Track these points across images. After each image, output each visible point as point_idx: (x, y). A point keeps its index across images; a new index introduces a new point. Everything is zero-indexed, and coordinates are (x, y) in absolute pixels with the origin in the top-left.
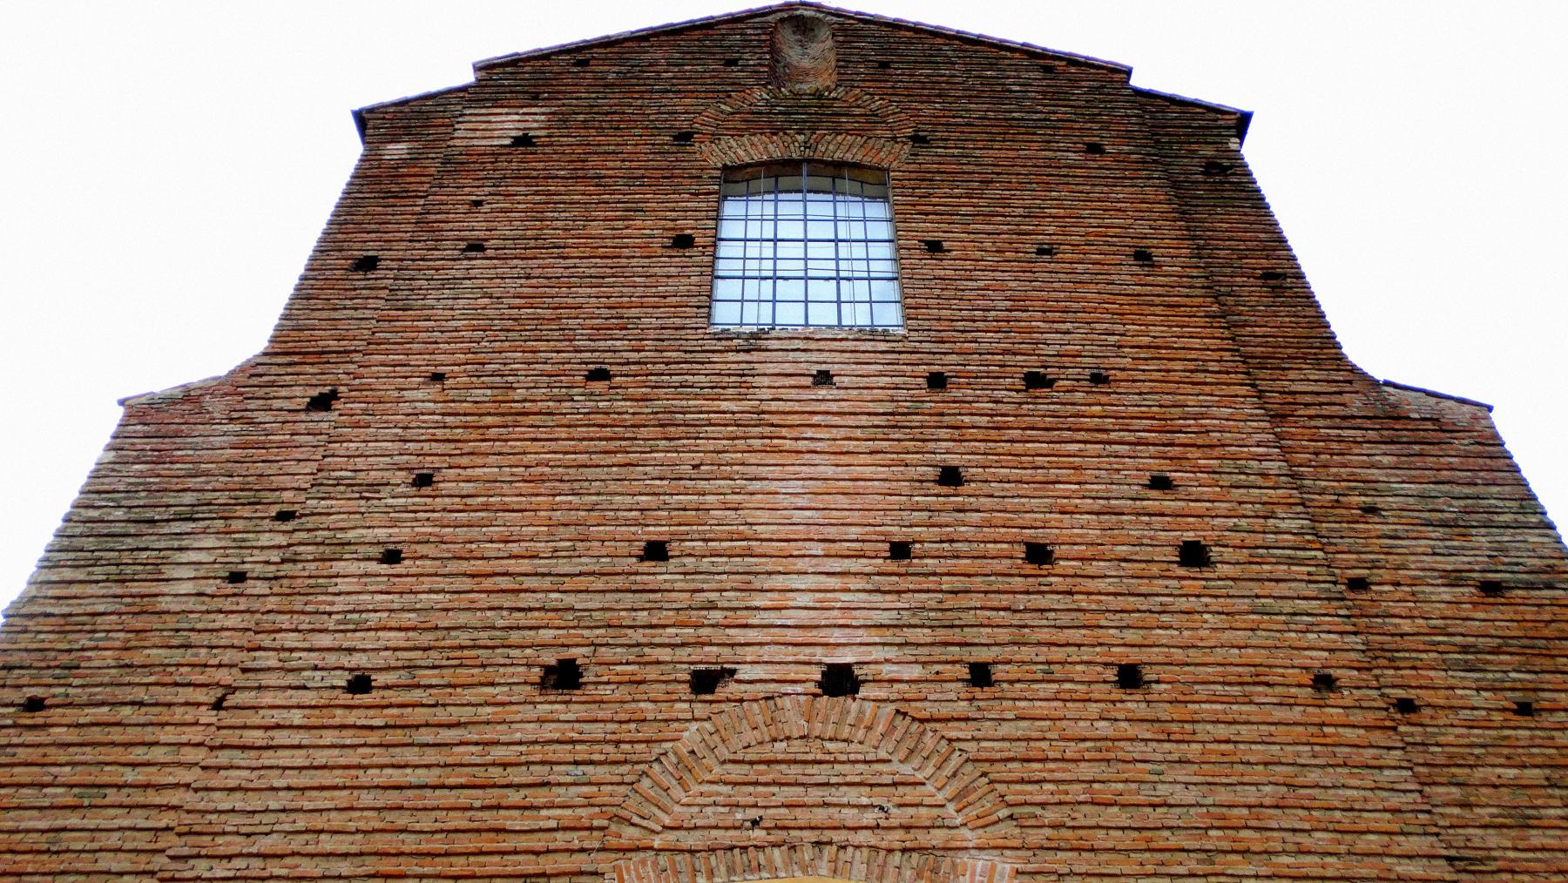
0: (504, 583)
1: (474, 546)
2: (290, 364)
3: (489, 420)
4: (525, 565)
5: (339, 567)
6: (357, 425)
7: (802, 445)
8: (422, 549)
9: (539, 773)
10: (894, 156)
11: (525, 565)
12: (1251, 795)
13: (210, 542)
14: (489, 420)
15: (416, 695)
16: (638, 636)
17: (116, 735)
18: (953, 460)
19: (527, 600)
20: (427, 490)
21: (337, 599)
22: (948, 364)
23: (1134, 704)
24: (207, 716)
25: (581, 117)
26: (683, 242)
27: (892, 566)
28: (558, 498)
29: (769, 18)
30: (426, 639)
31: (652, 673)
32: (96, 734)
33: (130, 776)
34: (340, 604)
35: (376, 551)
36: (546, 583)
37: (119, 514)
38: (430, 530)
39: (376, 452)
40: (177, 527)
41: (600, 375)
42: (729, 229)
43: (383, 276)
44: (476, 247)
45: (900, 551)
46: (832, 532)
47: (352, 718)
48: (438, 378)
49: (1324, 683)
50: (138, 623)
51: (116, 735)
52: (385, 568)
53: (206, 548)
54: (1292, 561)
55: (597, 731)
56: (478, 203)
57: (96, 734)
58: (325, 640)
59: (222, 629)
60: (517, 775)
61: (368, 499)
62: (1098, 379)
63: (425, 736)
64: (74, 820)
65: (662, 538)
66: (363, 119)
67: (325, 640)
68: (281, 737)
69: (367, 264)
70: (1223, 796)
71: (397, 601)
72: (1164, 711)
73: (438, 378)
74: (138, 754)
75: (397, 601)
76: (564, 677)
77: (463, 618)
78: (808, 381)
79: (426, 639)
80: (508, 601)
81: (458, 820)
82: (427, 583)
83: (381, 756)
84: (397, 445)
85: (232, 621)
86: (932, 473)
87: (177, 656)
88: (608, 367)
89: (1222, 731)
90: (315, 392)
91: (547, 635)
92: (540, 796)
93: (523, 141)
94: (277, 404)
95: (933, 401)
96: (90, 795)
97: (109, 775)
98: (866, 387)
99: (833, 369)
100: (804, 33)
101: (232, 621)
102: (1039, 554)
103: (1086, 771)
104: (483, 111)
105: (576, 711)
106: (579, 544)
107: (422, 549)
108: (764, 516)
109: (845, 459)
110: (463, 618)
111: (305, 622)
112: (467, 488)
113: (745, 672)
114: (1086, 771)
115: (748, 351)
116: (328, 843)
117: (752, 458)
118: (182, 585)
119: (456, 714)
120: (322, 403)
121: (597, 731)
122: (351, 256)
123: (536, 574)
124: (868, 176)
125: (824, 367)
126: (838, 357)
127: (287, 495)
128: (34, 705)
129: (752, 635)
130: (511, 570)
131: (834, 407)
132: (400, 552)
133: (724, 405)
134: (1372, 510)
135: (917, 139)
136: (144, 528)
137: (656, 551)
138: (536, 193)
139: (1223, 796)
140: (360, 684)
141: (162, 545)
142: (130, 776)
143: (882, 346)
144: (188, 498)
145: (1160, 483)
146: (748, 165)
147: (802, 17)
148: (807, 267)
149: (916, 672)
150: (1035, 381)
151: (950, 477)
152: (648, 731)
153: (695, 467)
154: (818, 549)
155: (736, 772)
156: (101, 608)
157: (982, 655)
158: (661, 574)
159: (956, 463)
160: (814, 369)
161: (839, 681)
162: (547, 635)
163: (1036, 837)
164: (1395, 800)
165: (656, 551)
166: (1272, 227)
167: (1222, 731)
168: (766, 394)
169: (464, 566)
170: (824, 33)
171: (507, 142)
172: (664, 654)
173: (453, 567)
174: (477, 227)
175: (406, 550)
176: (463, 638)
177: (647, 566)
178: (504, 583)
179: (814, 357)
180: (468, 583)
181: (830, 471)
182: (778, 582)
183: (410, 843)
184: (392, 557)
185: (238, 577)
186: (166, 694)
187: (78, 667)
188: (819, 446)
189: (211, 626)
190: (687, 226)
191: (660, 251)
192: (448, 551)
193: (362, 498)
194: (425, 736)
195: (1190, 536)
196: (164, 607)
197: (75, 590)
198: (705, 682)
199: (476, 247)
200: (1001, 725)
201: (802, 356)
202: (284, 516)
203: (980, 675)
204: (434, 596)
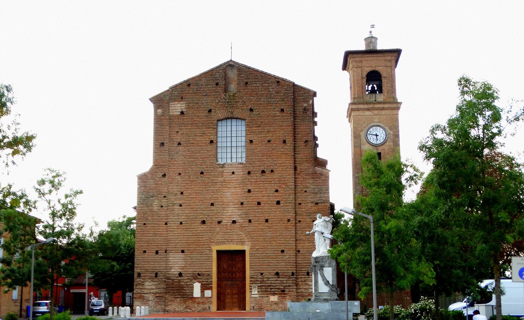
0: (194, 209)
3: (188, 182)
4: (197, 207)
6: (171, 183)
7: (230, 186)
9: (202, 234)
11: (197, 207)
12: (277, 235)
14: (188, 182)
15: (187, 225)
16: (211, 217)
17: (155, 228)
18: (250, 188)
19: (198, 212)
23: (266, 224)
24: (165, 226)
25: (191, 105)
26: (212, 142)
27: (241, 206)
30: (187, 217)
31: (213, 222)
32: (153, 228)
33: (159, 233)
34: (177, 212)
36: (200, 209)
39: (176, 189)
40: (152, 198)
41: (202, 173)
42: (219, 134)
43: (166, 146)
45: (242, 204)
46: (233, 201)
47: (182, 227)
48: (180, 174)
49: (289, 220)
50: (152, 213)
51: (155, 228)
53: (156, 203)
54: (290, 203)
55: (208, 229)
56: (178, 132)
57: (153, 228)
58: (176, 217)
60: (200, 234)
62: (272, 171)
63: (190, 230)
64: (154, 238)
66: (150, 99)
67: (176, 217)
68: (175, 230)
69: (162, 144)
70: (274, 235)
71: (183, 212)
72: (269, 225)
74: (159, 230)
75: (183, 212)
76: (204, 222)
77: (191, 214)
78: (231, 174)
79: (187, 217)
80: (196, 212)
81: (195, 239)
83: (186, 232)
85: (163, 213)
86: (247, 190)
87: (158, 218)
89: (275, 227)
91: (201, 217)
92: (202, 237)
93: (182, 113)
95: (248, 177)
96: (155, 235)
97: (156, 233)
101: (163, 213)
102: (259, 203)
103: (260, 232)
105: (205, 227)
110: (191, 214)
111: (173, 215)
113: (224, 221)
114: (260, 232)
116: (182, 242)
117: (224, 189)
118: (155, 208)
119: (192, 227)
121: (208, 229)
122: (160, 145)
126: (235, 168)
128: (145, 224)
129: (224, 217)
133: (220, 179)
134: (306, 191)
135: (251, 110)
137: (212, 204)
139: (274, 235)
140: (181, 223)
142: (159, 233)
143: (242, 166)
145: (277, 191)
148: (232, 142)
149: (242, 221)
150: (263, 172)
151: (249, 191)
152: (213, 229)
154: (232, 204)
155: (222, 234)
157: (250, 218)
158: (213, 208)
161: (234, 222)
162: (201, 217)
163: (253, 240)
164: (292, 235)
165: (212, 204)
167: (275, 227)
169: (189, 207)
172: (214, 219)
174: (178, 138)
176: (191, 217)
177: (212, 207)
178: (194, 209)
179: (232, 169)
180: (190, 209)
181: (233, 191)
182: (227, 209)
183: (191, 242)
184: (181, 206)
185: (162, 206)
186: (159, 223)
190: (212, 138)
194: (190, 230)
195: (278, 200)
198: (219, 222)
199: (179, 144)
200: (251, 228)
202: (165, 197)
203: (250, 221)
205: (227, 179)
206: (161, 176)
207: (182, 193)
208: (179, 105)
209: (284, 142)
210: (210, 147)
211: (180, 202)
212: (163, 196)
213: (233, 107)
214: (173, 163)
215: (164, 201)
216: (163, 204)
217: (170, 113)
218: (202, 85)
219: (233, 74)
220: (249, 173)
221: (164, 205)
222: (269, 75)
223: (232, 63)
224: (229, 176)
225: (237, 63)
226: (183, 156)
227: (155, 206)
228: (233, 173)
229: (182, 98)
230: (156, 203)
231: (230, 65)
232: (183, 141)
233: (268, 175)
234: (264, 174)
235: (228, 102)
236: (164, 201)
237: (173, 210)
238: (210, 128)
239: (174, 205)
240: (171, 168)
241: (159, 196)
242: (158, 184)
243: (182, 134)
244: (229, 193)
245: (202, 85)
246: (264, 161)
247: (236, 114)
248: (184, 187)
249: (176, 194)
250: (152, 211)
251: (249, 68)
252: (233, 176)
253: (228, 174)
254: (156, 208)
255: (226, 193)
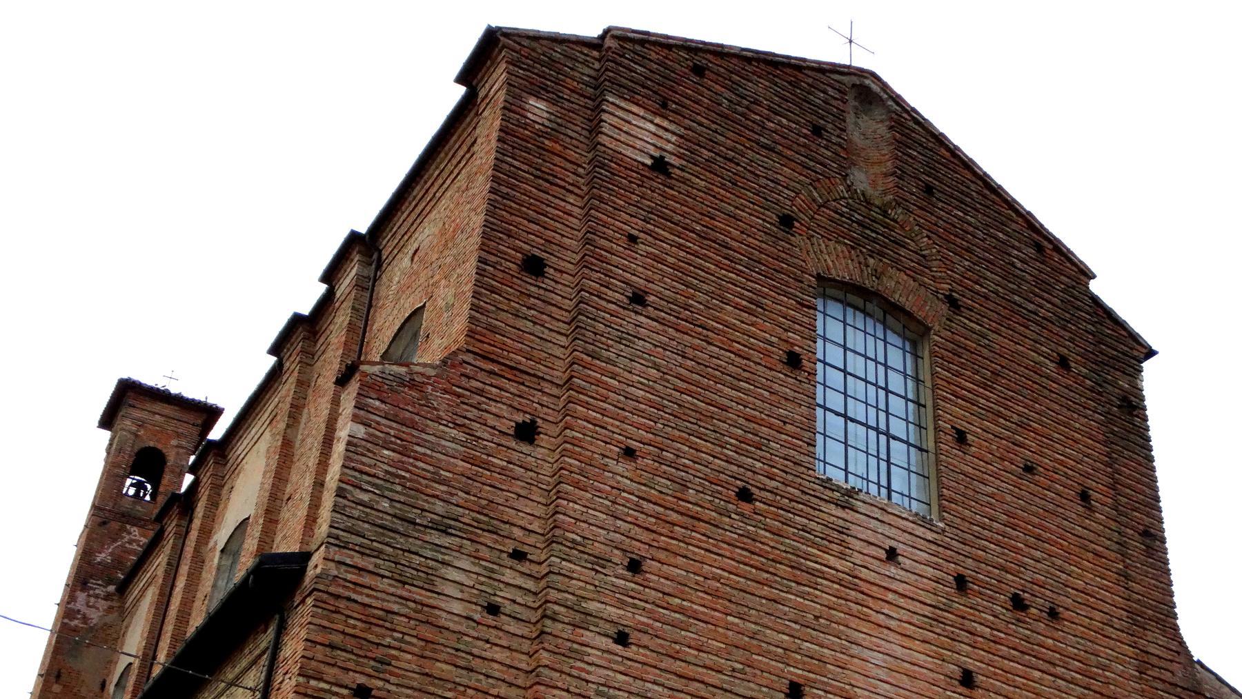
1: (678, 647)
2: (491, 372)
3: (674, 517)
4: (714, 678)
5: (587, 636)
6: (576, 484)
8: (645, 640)
10: (932, 311)
11: (714, 678)
13: (465, 564)
14: (674, 517)
18: (971, 664)
20: (638, 578)
21: (592, 669)
22: (968, 567)
28: (729, 618)
29: (845, 79)
35: (612, 630)
37: (385, 504)
38: (645, 620)
41: (745, 495)
44: (638, 299)
48: (629, 453)
52: (618, 648)
56: (633, 239)
59: (492, 660)
61: (597, 571)
65: (801, 681)
73: (629, 453)
82: (652, 674)
84: (610, 520)
85: (499, 655)
88: (754, 490)
90: (520, 418)
93: (660, 165)
94: (491, 421)
98: (919, 572)
99: (900, 548)
100: (861, 102)
104: (623, 104)
106: (748, 669)
107: (645, 640)
108: (859, 680)
109: (907, 642)
112: (668, 586)
115: (843, 508)
117: (854, 623)
118: (454, 606)
120: (526, 432)
123: (721, 689)
124: (913, 326)
125: (893, 544)
127: (517, 532)
130: (706, 679)
131: (900, 588)
132: (627, 635)
133: (832, 561)
136: (410, 530)
138: (680, 246)
141: (429, 554)
143: (930, 536)
144: (439, 507)
146: (834, 280)
147: (868, 88)
153: (817, 618)
156: (396, 608)
159: (971, 668)
160: (888, 543)
166: (1155, 489)
168: (858, 559)
170: (878, 113)
171: (649, 162)
173: (666, 663)
174: (635, 268)
175: (634, 636)
179: (892, 532)
181: (899, 651)
184: (622, 639)
185: (493, 609)
187: (389, 664)
188: (893, 624)
189: (484, 654)
191: (780, 367)
192: (662, 646)
193: (593, 569)
196: (442, 622)
197: (367, 580)
199: (638, 299)
201: (881, 528)
202: (518, 555)
204: (656, 687)
205: (864, 573)
206: (508, 426)
207: (635, 566)
208: (652, 128)
209: (1084, 497)
210: (784, 382)
211: (628, 617)
212: (510, 546)
213: (882, 255)
214: (598, 383)
215: (508, 576)
216: (503, 596)
217: (603, 139)
218: (756, 102)
219: (866, 130)
220: (961, 583)
221: (508, 607)
222: (1011, 205)
223: (875, 88)
224: (875, 564)
225: (898, 100)
226: (657, 367)
227: (450, 590)
228: (892, 554)
229: (664, 106)
230: (460, 574)
231: (864, 90)
232: (660, 288)
233: (1036, 628)
234: (1021, 615)
235: (859, 223)
236: (508, 576)
237: (573, 654)
238: (786, 294)
239: (585, 620)
240: (586, 405)
241: (488, 538)
242: (487, 466)
243: (656, 259)
244: (878, 658)
245: (756, 102)
246: (1017, 551)
247: (897, 286)
248: (645, 536)
249: (600, 562)
250: (425, 616)
251: (940, 139)
252: (893, 570)
253: (873, 551)
254: (457, 608)
255: (866, 654)
